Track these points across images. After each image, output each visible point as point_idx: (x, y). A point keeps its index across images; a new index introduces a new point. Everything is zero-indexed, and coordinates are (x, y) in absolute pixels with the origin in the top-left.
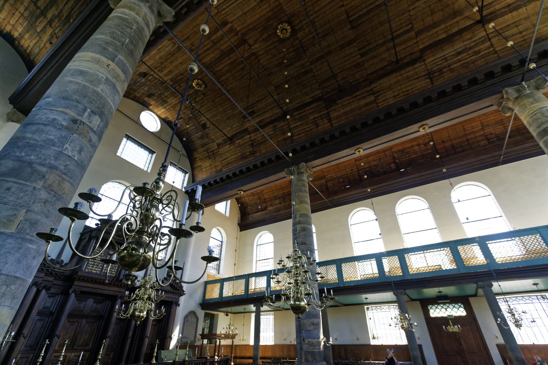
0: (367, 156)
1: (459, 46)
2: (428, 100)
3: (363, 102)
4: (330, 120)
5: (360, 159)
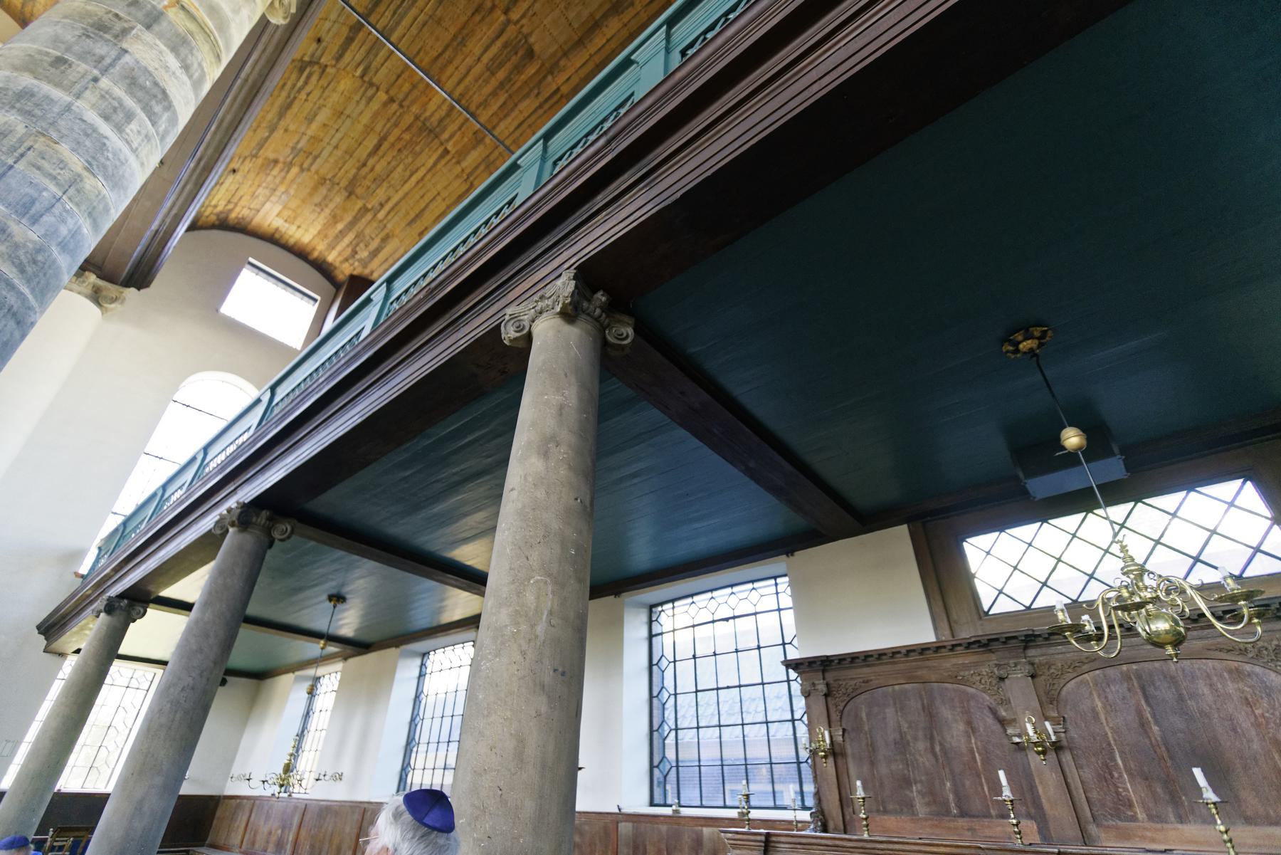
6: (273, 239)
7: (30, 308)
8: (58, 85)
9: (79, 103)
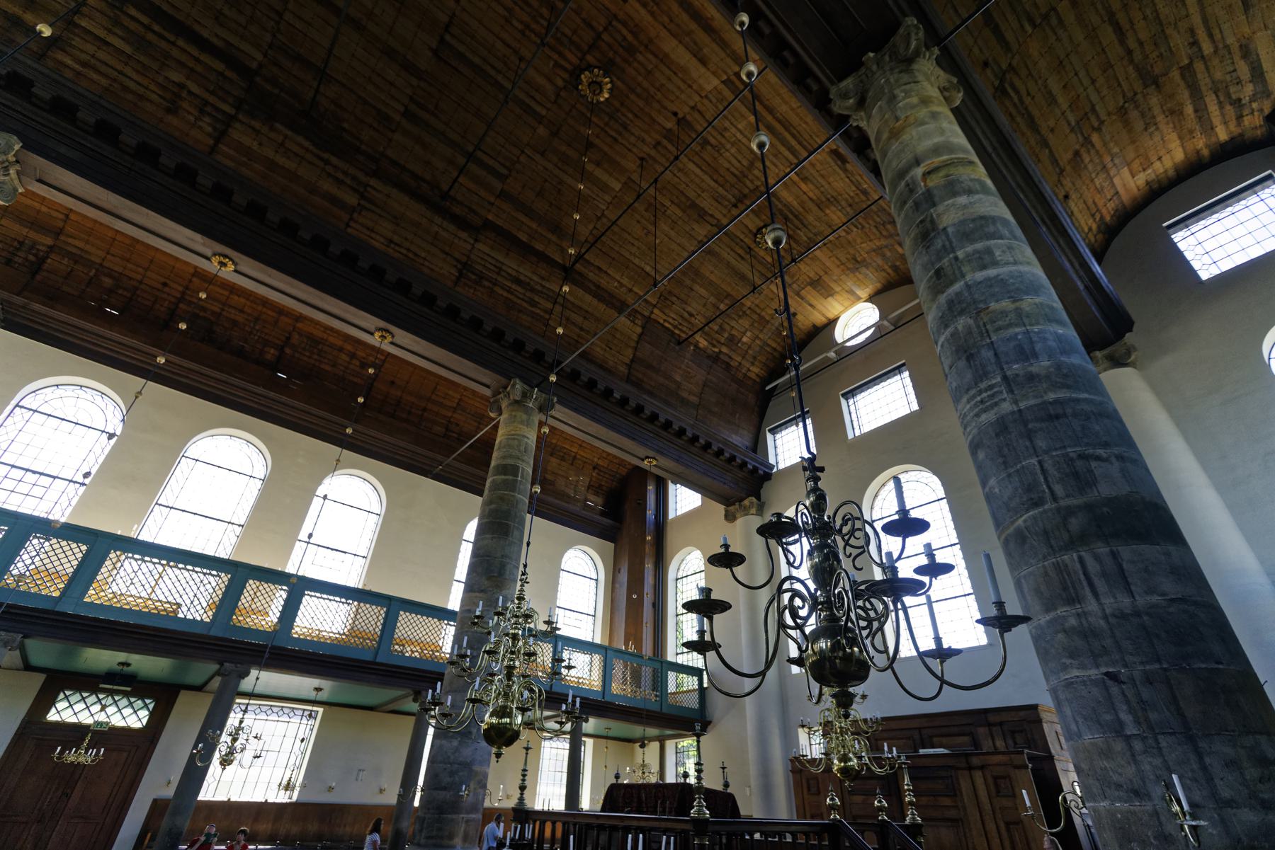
0: (232, 288)
1: (526, 272)
2: (428, 300)
3: (327, 186)
4: (220, 136)
5: (209, 280)
6: (1156, 192)
7: (1101, 403)
8: (952, 283)
9: (968, 278)
